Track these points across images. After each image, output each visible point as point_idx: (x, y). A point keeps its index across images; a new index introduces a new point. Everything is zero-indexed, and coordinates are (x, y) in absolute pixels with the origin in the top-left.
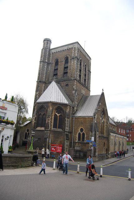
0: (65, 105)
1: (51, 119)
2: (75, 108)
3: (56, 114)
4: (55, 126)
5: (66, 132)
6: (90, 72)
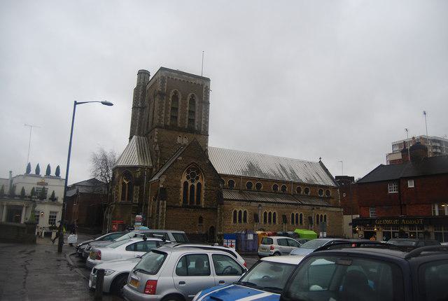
0: (135, 168)
2: (154, 170)
4: (123, 198)
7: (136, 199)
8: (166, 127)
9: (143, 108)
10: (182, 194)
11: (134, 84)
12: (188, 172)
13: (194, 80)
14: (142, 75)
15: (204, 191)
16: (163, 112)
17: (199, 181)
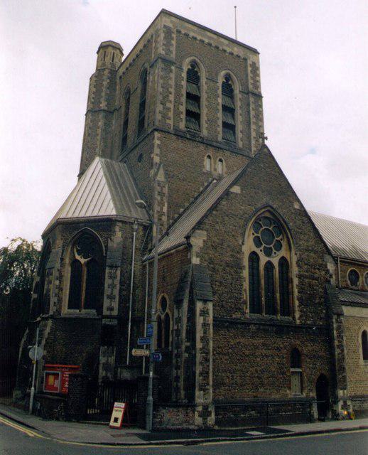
0: (106, 224)
1: (60, 278)
3: (78, 257)
5: (107, 317)
6: (259, 97)
7: (111, 305)
8: (179, 135)
9: (109, 113)
10: (246, 285)
11: (91, 66)
12: (257, 225)
13: (227, 45)
14: (110, 50)
15: (296, 281)
16: (172, 97)
17: (283, 252)
